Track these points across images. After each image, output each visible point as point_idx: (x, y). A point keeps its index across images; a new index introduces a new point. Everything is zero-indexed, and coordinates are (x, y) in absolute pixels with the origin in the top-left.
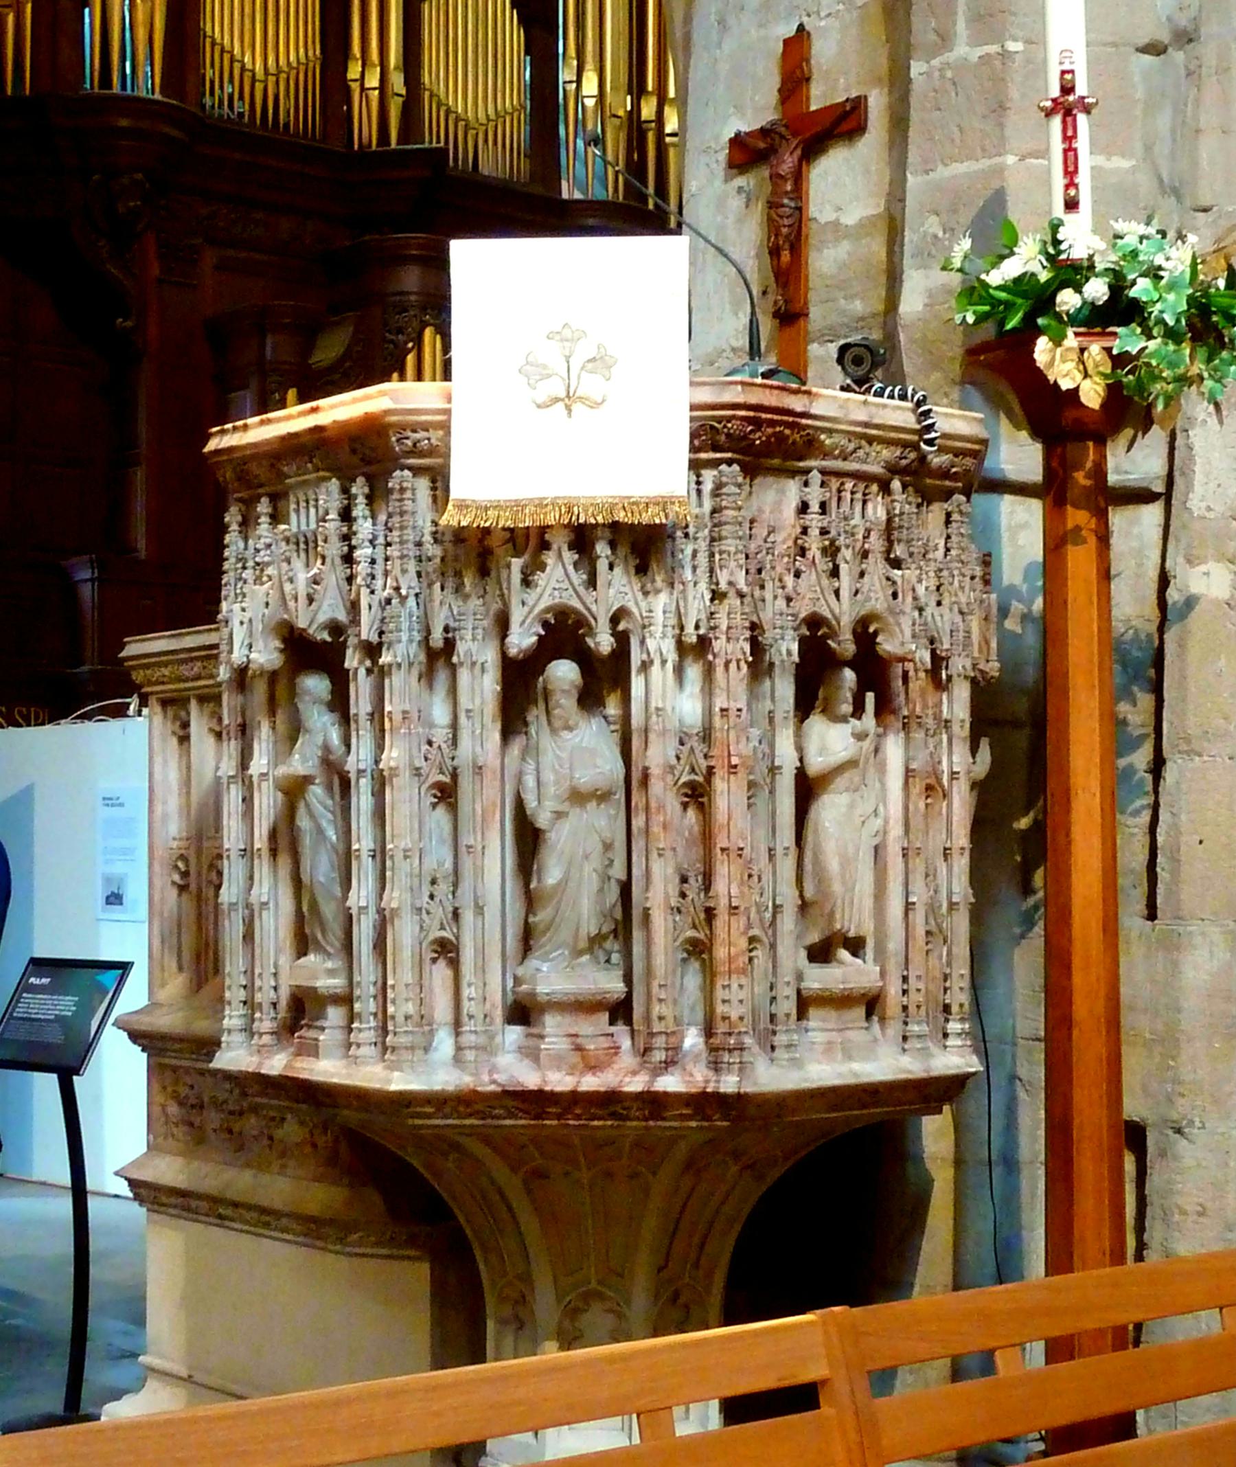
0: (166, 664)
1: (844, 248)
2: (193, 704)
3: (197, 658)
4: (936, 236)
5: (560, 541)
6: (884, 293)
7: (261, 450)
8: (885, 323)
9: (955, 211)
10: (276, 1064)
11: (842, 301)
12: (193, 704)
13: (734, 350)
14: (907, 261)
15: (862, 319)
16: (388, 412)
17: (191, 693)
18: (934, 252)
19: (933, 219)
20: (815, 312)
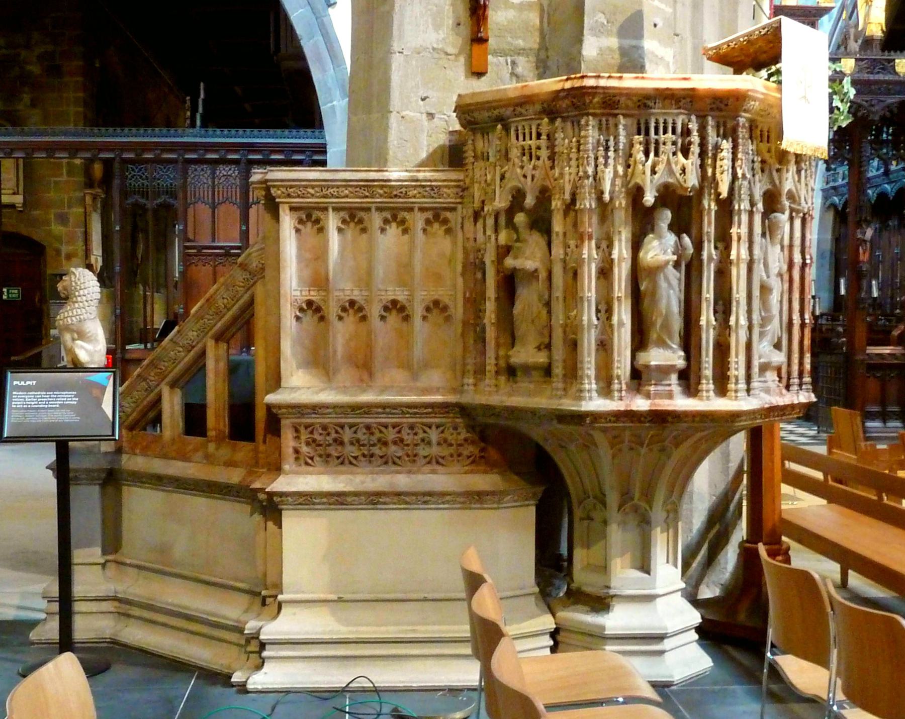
0: (333, 187)
1: (511, 14)
2: (330, 210)
3: (351, 186)
4: (603, 24)
5: (793, 160)
6: (538, 40)
7: (639, 92)
8: (538, 55)
9: (614, 14)
10: (641, 404)
11: (509, 39)
12: (330, 210)
13: (434, 49)
14: (586, 32)
15: (524, 49)
16: (748, 90)
17: (331, 205)
18: (602, 30)
19: (601, 15)
20: (491, 41)
